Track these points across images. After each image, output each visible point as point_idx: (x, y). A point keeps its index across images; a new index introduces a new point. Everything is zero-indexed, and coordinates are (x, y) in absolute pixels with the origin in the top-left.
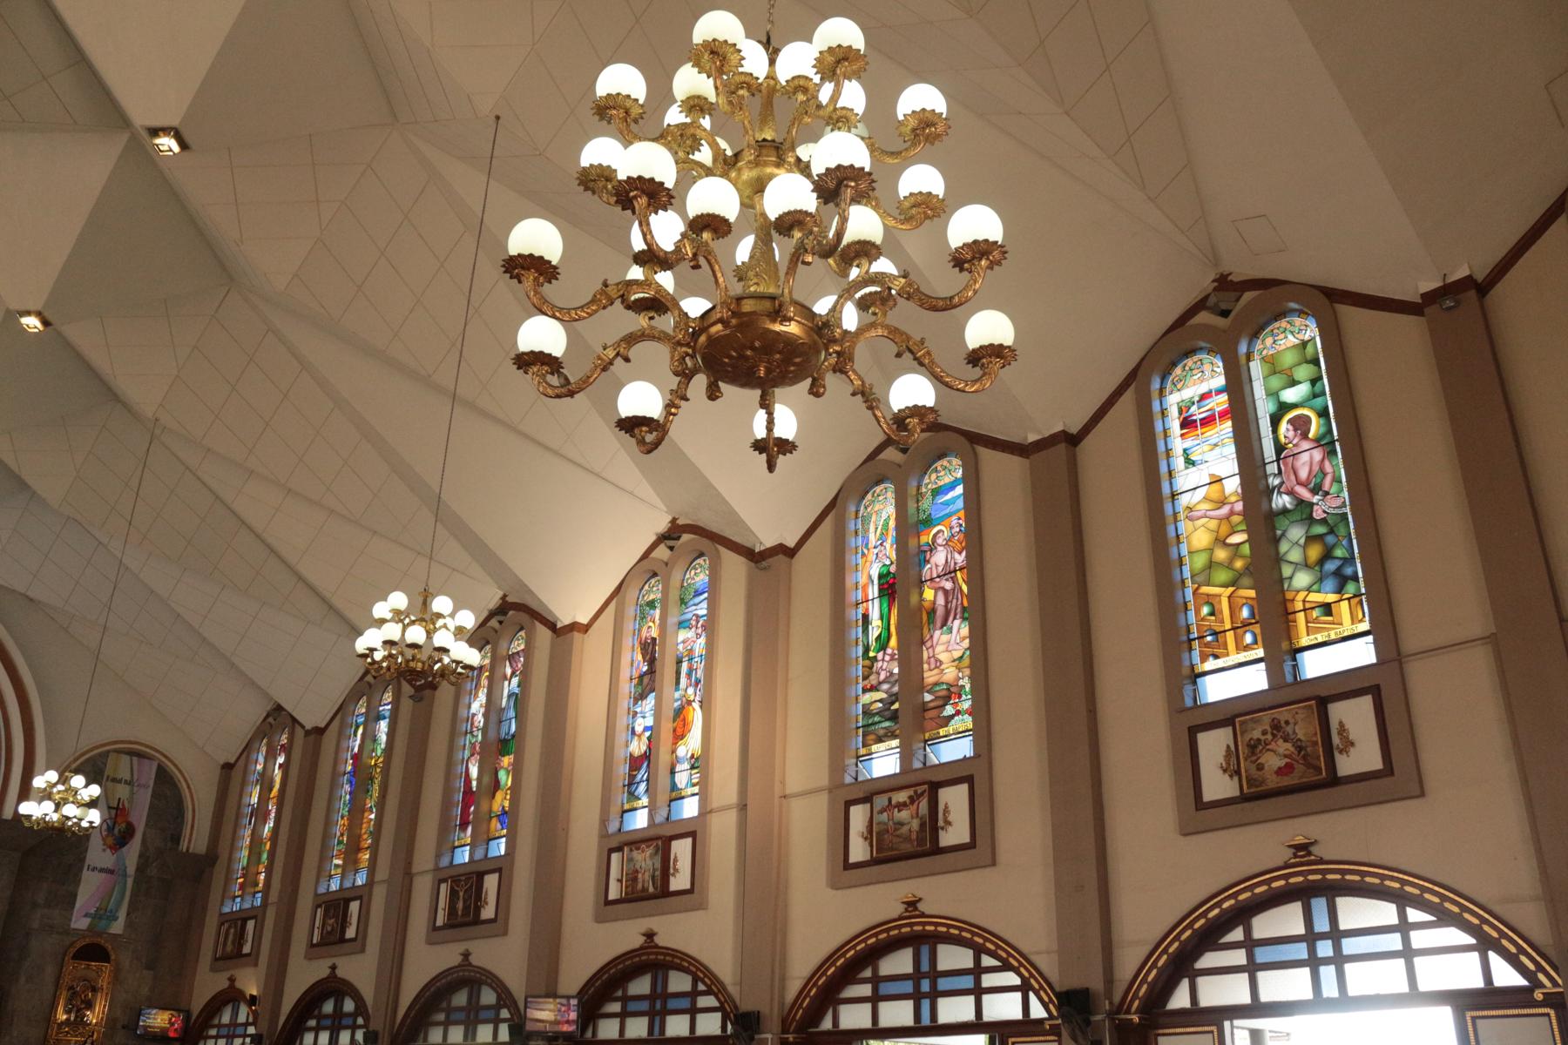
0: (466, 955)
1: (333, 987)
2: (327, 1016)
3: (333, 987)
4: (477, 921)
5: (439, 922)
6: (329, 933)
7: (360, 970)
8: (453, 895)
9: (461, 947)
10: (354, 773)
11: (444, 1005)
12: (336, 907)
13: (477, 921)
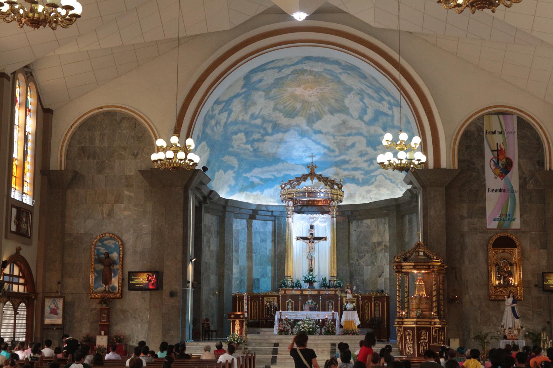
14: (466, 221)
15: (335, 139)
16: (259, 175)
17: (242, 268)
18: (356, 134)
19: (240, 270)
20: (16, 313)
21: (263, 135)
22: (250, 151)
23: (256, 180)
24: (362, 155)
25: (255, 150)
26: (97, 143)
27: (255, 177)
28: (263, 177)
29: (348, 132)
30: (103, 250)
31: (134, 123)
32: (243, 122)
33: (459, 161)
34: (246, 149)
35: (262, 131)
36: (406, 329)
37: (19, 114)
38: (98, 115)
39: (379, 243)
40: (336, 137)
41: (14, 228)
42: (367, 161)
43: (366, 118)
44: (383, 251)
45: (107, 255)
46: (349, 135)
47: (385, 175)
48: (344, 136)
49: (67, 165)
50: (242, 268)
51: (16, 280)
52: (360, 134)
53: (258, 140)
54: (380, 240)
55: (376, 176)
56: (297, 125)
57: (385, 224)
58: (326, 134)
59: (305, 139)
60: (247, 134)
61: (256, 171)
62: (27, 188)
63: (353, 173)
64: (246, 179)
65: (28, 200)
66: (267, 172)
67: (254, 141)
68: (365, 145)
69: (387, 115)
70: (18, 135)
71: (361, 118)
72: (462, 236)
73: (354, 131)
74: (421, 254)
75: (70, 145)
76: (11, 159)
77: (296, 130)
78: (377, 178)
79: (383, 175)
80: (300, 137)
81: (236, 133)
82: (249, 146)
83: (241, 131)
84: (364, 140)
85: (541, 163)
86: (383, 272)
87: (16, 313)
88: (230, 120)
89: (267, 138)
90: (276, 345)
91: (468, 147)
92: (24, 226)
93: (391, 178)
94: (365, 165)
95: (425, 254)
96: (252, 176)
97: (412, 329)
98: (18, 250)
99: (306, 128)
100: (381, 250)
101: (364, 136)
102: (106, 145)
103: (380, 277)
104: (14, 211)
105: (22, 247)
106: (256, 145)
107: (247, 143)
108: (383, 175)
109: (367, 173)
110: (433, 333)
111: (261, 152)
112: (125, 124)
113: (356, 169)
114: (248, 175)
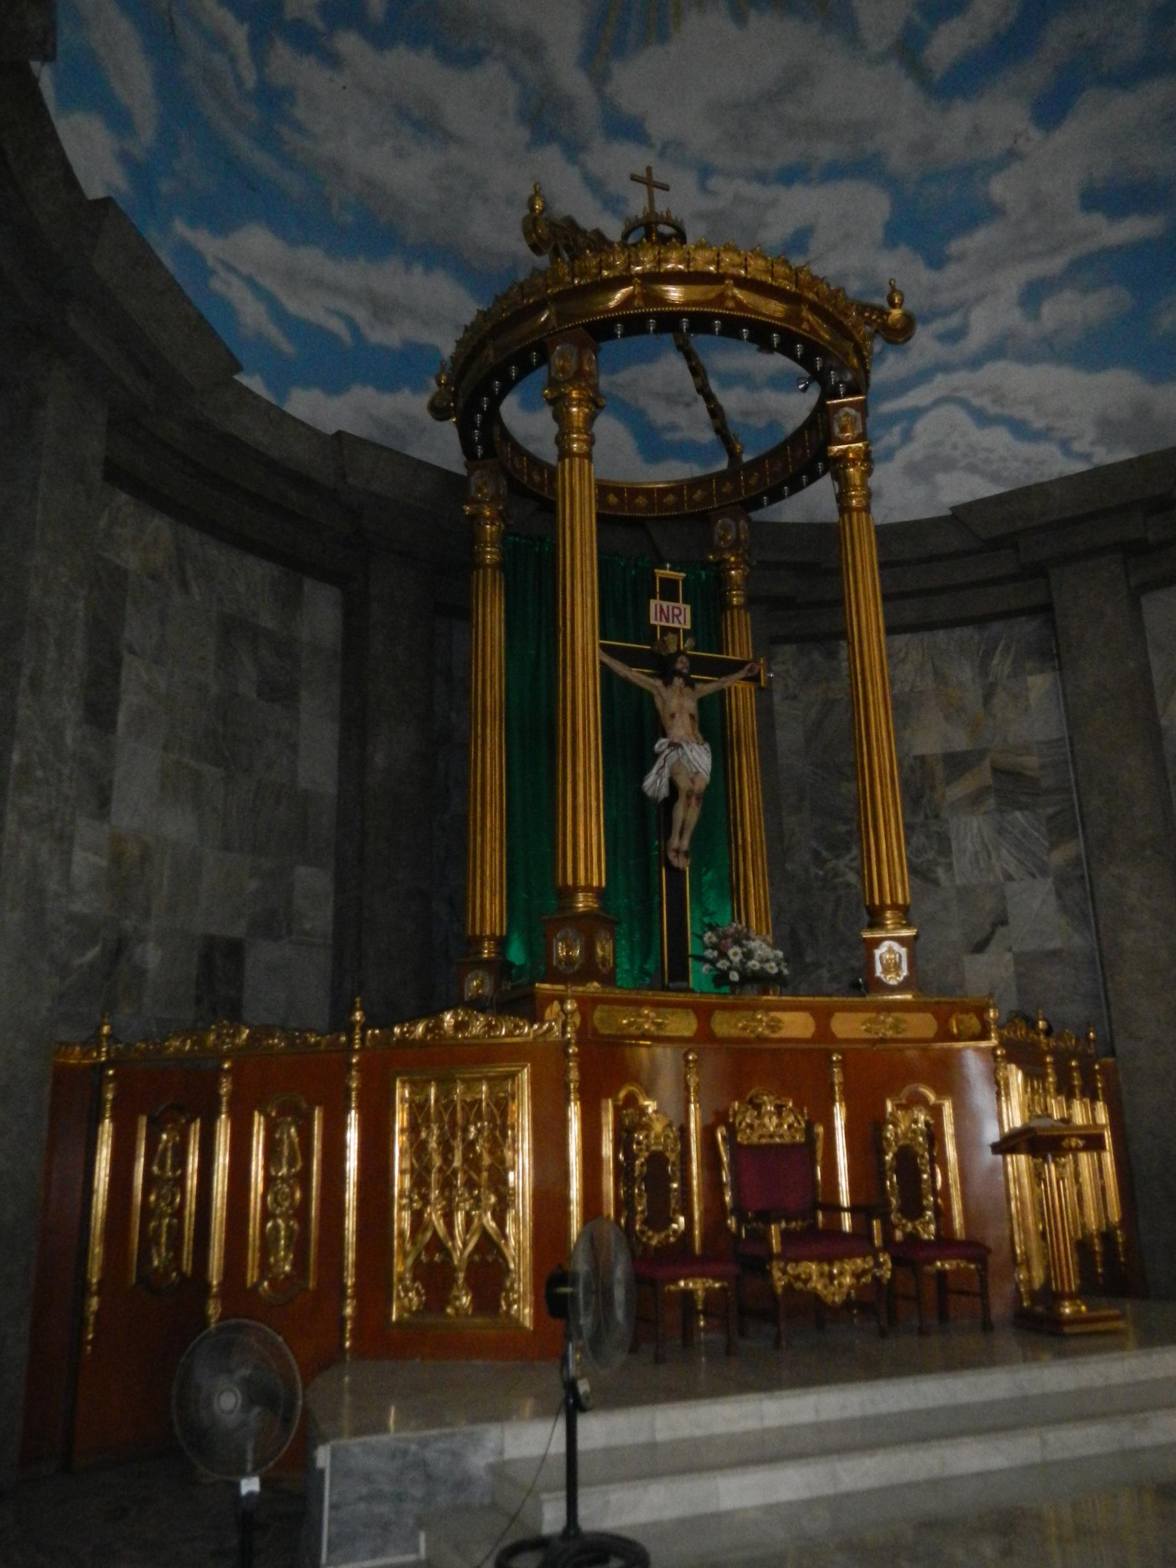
15: (703, 188)
16: (267, 282)
17: (132, 850)
18: (833, 173)
19: (117, 859)
22: (240, 83)
27: (250, 281)
28: (292, 306)
34: (219, 42)
40: (714, 182)
43: (948, 44)
44: (991, 802)
46: (790, 176)
47: (977, 402)
48: (761, 178)
50: (132, 850)
52: (863, 167)
53: (305, 39)
54: (960, 741)
55: (915, 414)
56: (533, 47)
57: (988, 655)
58: (662, 154)
59: (551, 155)
61: (257, 243)
66: (318, 283)
68: (879, 233)
71: (908, 50)
73: (826, 151)
77: (514, 73)
78: (920, 426)
79: (964, 404)
80: (524, 134)
84: (873, 205)
86: (1001, 921)
89: (348, 43)
93: (1027, 413)
96: (230, 268)
99: (573, 80)
100: (975, 799)
101: (891, 183)
103: (980, 947)
108: (964, 404)
111: (298, 127)
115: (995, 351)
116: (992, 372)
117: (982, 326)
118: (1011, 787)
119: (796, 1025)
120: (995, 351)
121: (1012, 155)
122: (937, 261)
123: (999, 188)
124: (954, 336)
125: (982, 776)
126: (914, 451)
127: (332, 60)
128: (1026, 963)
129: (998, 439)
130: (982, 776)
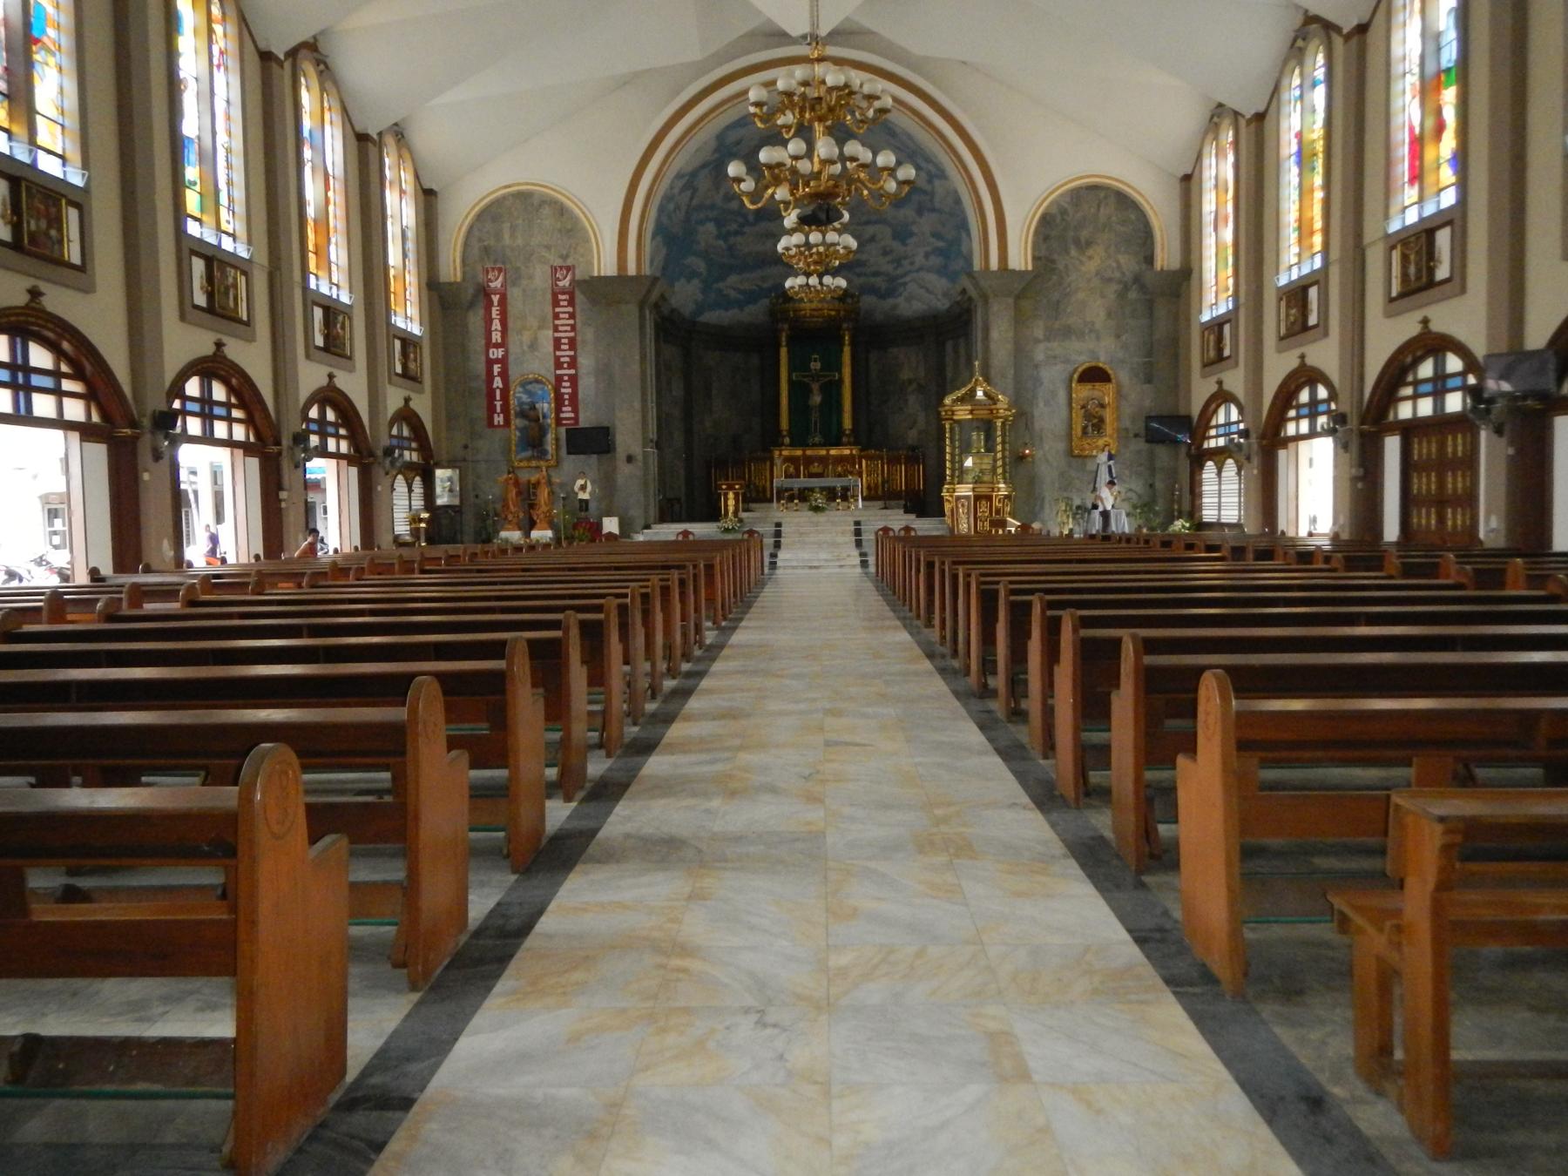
0: (1425, 321)
1: (1307, 376)
2: (1304, 405)
3: (1307, 376)
4: (1431, 284)
5: (1394, 294)
6: (1293, 323)
7: (1325, 354)
8: (1405, 259)
9: (1418, 315)
10: (1300, 153)
11: (1410, 378)
12: (1297, 294)
13: (1431, 284)
14: (1041, 346)
18: (876, 222)
20: (410, 491)
21: (742, 226)
23: (733, 294)
24: (885, 253)
25: (730, 248)
26: (507, 240)
29: (864, 219)
30: (525, 398)
31: (561, 211)
32: (712, 207)
33: (1035, 258)
35: (740, 220)
36: (958, 498)
37: (391, 197)
38: (504, 197)
39: (910, 382)
41: (399, 369)
42: (891, 262)
45: (533, 408)
46: (868, 223)
49: (464, 273)
51: (406, 444)
53: (736, 233)
60: (719, 223)
61: (733, 279)
62: (413, 310)
63: (873, 280)
64: (720, 291)
65: (415, 329)
67: (729, 233)
69: (925, 192)
70: (393, 230)
72: (1036, 366)
74: (980, 394)
75: (466, 245)
76: (386, 267)
81: (702, 222)
82: (721, 242)
83: (708, 219)
84: (888, 231)
85: (1150, 260)
87: (410, 491)
88: (695, 202)
89: (747, 229)
90: (779, 525)
91: (1046, 238)
92: (412, 366)
94: (889, 268)
95: (985, 394)
97: (967, 497)
98: (407, 400)
102: (520, 241)
104: (398, 344)
105: (413, 395)
106: (732, 240)
107: (718, 237)
109: (892, 279)
110: (996, 503)
112: (546, 211)
113: (876, 274)
114: (721, 285)
115: (921, 269)
116: (923, 274)
117: (919, 260)
118: (921, 389)
119: (823, 452)
120: (921, 269)
121: (914, 223)
122: (905, 244)
123: (915, 229)
124: (912, 263)
125: (914, 385)
126: (905, 294)
127: (743, 234)
128: (920, 433)
129: (922, 291)
130: (914, 385)
